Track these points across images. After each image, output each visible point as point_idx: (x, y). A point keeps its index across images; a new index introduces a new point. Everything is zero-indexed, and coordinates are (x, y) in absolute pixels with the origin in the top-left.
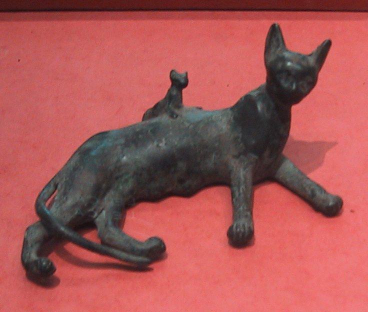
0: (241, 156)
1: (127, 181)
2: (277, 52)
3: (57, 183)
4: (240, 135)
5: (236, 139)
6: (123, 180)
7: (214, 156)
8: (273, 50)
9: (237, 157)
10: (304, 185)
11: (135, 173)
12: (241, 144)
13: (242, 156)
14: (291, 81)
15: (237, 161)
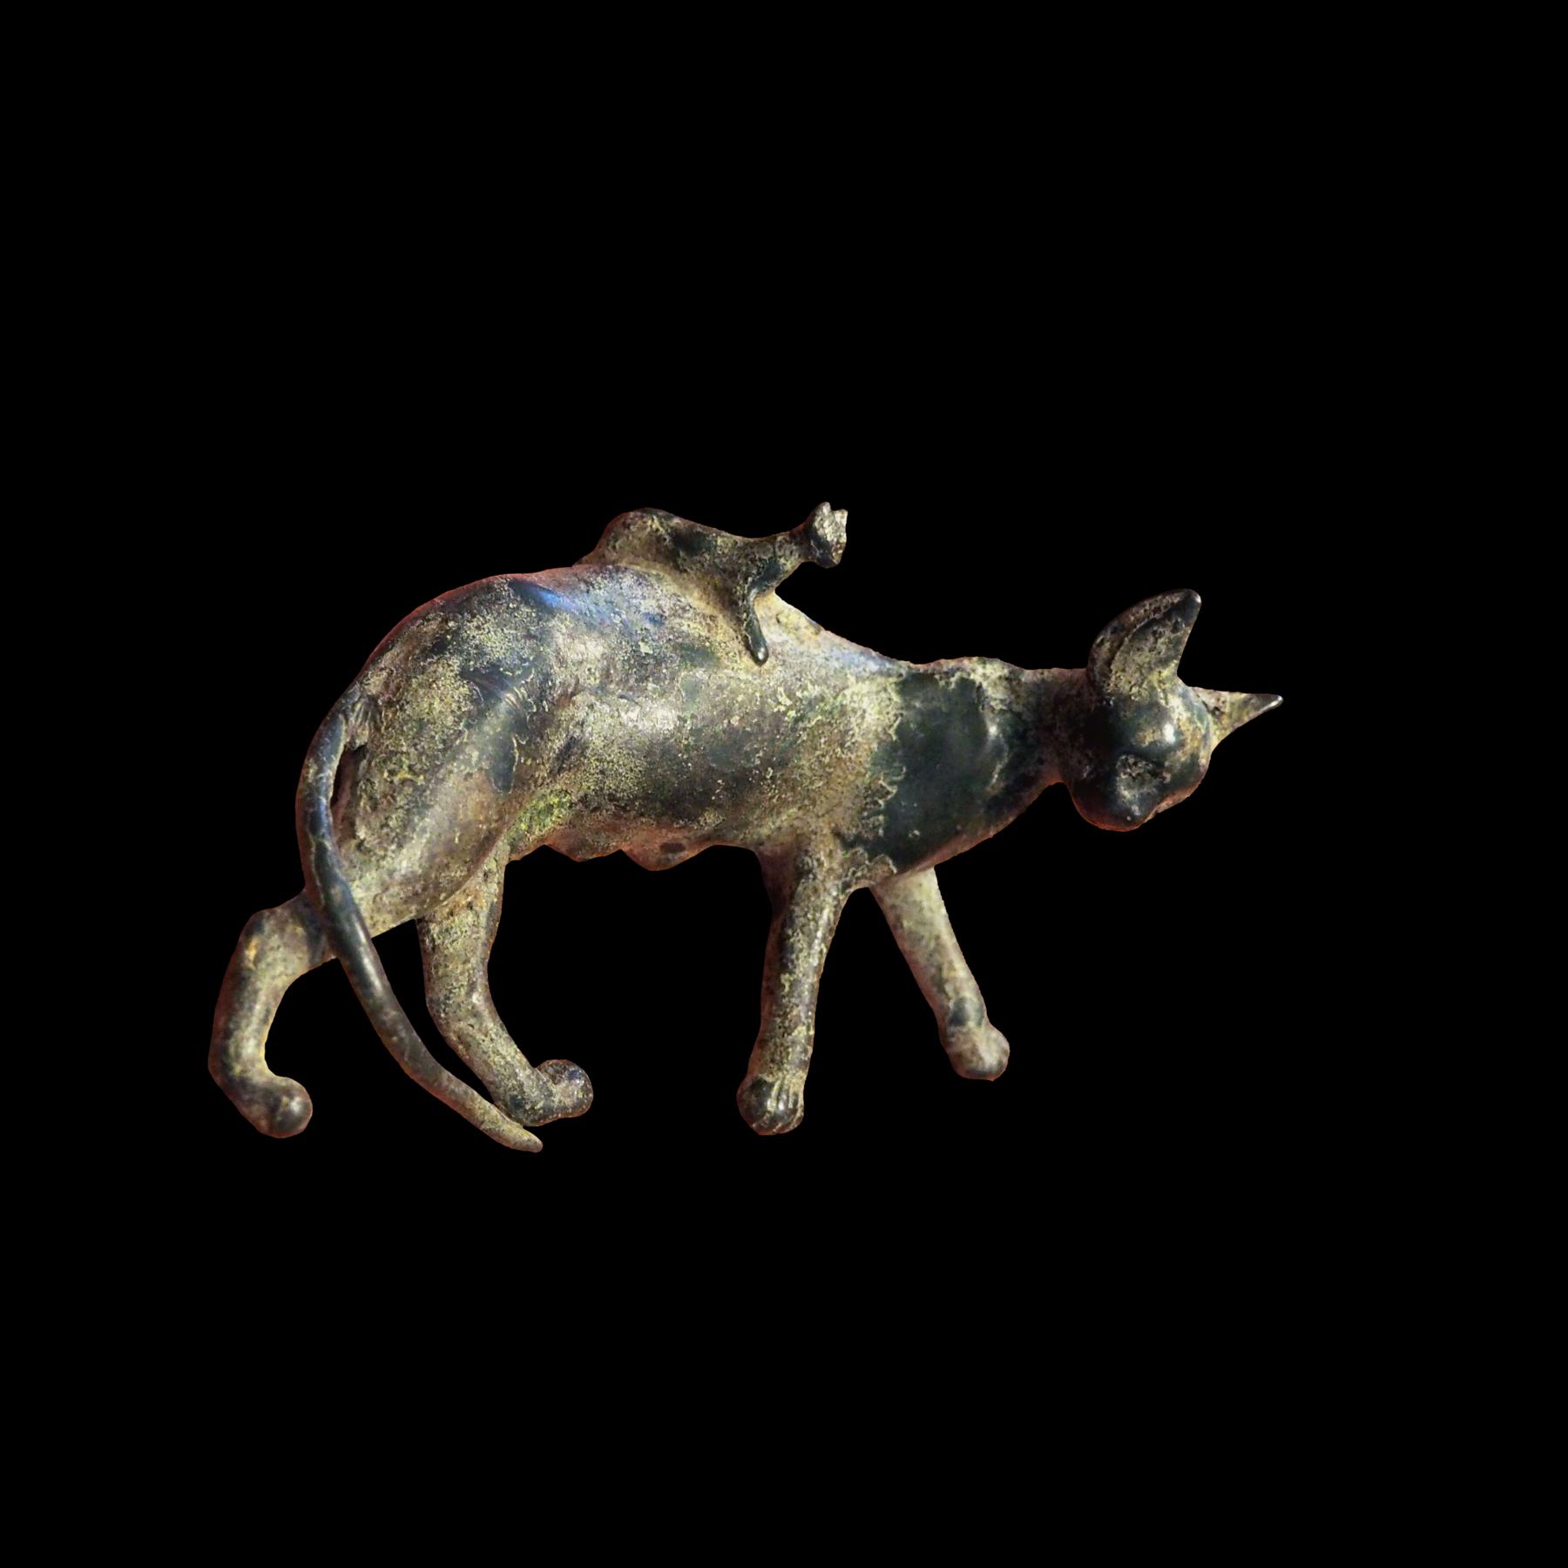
0: (860, 850)
1: (549, 809)
2: (1154, 677)
3: (358, 742)
4: (894, 790)
5: (873, 792)
6: (542, 805)
7: (793, 810)
8: (1144, 657)
9: (848, 845)
10: (945, 974)
11: (584, 800)
12: (881, 818)
13: (860, 850)
14: (1145, 790)
15: (840, 854)
